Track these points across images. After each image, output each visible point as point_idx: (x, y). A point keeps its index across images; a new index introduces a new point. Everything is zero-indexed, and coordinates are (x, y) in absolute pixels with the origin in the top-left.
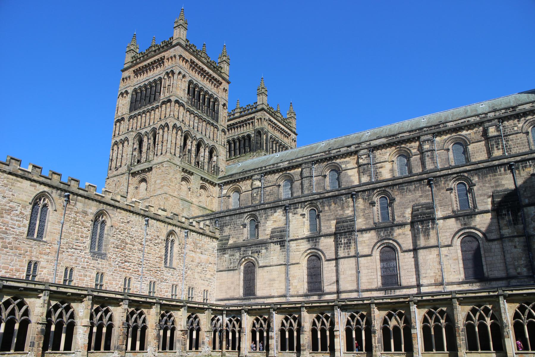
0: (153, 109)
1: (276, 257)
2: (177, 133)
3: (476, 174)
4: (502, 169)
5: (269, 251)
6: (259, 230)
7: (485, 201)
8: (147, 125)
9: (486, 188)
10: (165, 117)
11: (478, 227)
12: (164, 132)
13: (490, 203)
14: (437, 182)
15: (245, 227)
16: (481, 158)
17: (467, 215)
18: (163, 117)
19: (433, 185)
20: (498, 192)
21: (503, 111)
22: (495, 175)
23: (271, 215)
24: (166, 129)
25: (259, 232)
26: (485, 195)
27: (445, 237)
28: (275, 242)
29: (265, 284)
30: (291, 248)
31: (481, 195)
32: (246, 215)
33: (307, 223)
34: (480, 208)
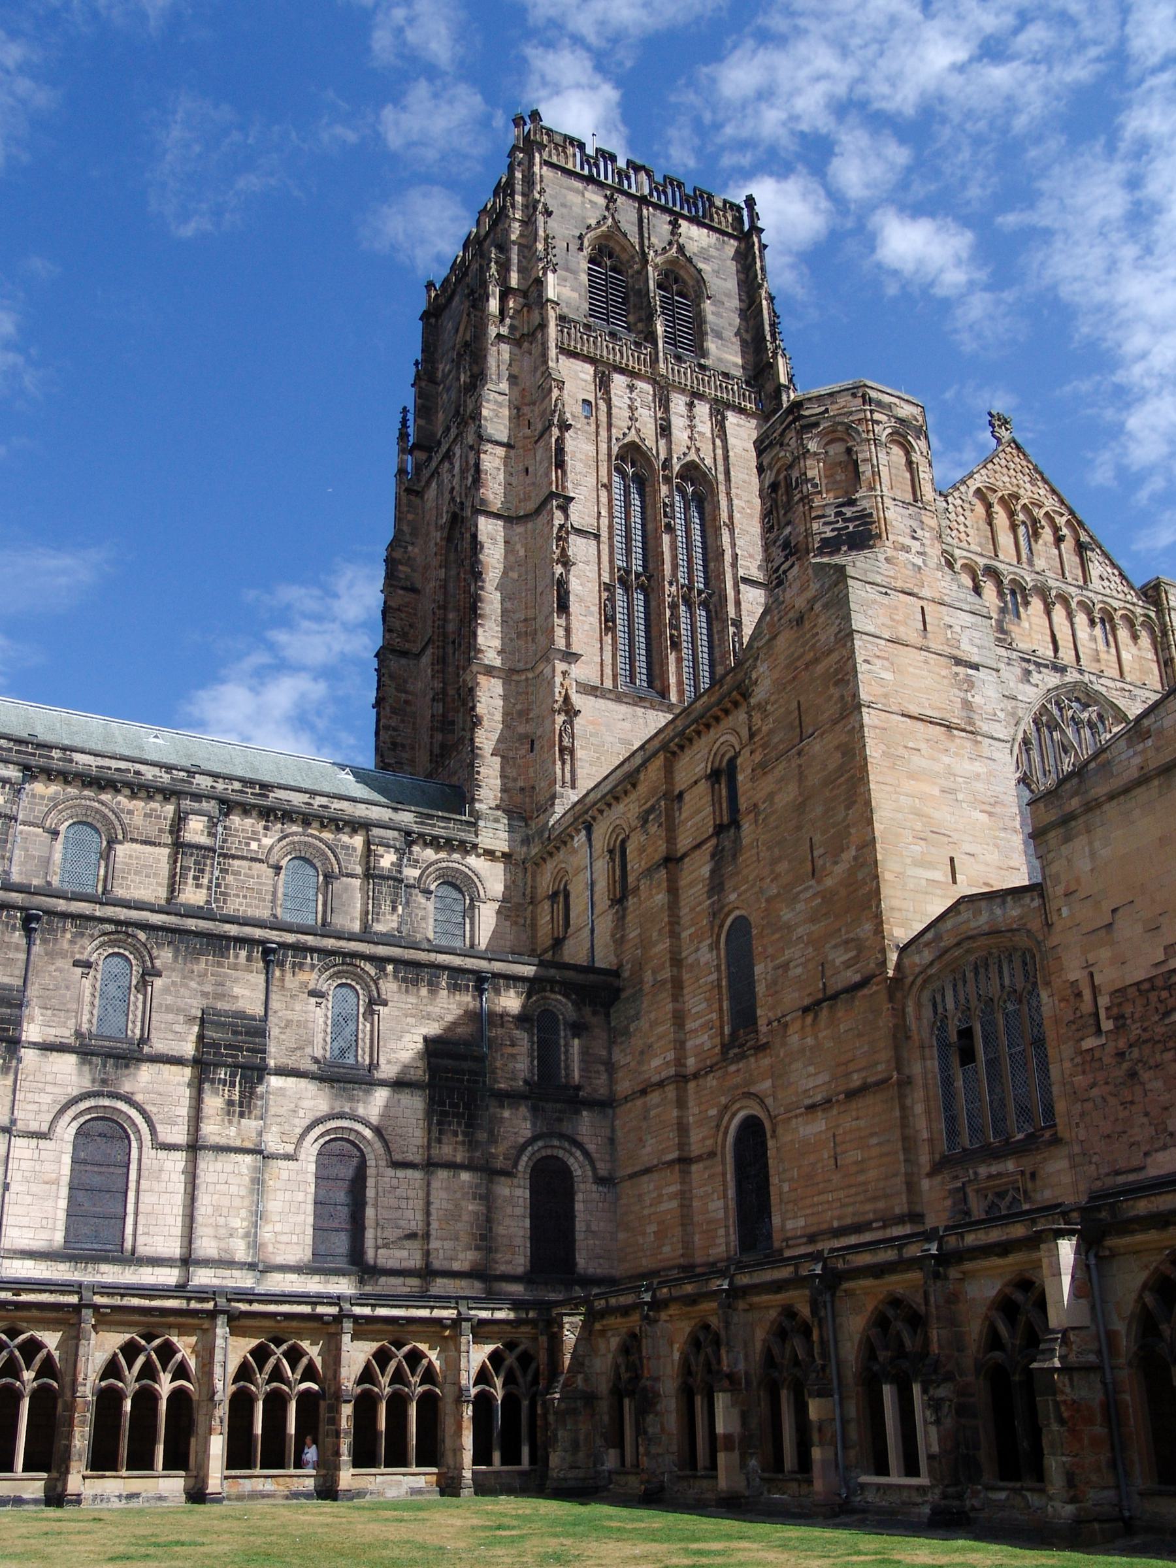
3: (170, 943)
4: (243, 954)
7: (177, 1028)
9: (186, 993)
11: (139, 1098)
13: (193, 1038)
14: (52, 931)
17: (117, 1057)
19: (37, 936)
20: (218, 1013)
26: (179, 1011)
27: (35, 1107)
31: (169, 1009)
34: (159, 1045)
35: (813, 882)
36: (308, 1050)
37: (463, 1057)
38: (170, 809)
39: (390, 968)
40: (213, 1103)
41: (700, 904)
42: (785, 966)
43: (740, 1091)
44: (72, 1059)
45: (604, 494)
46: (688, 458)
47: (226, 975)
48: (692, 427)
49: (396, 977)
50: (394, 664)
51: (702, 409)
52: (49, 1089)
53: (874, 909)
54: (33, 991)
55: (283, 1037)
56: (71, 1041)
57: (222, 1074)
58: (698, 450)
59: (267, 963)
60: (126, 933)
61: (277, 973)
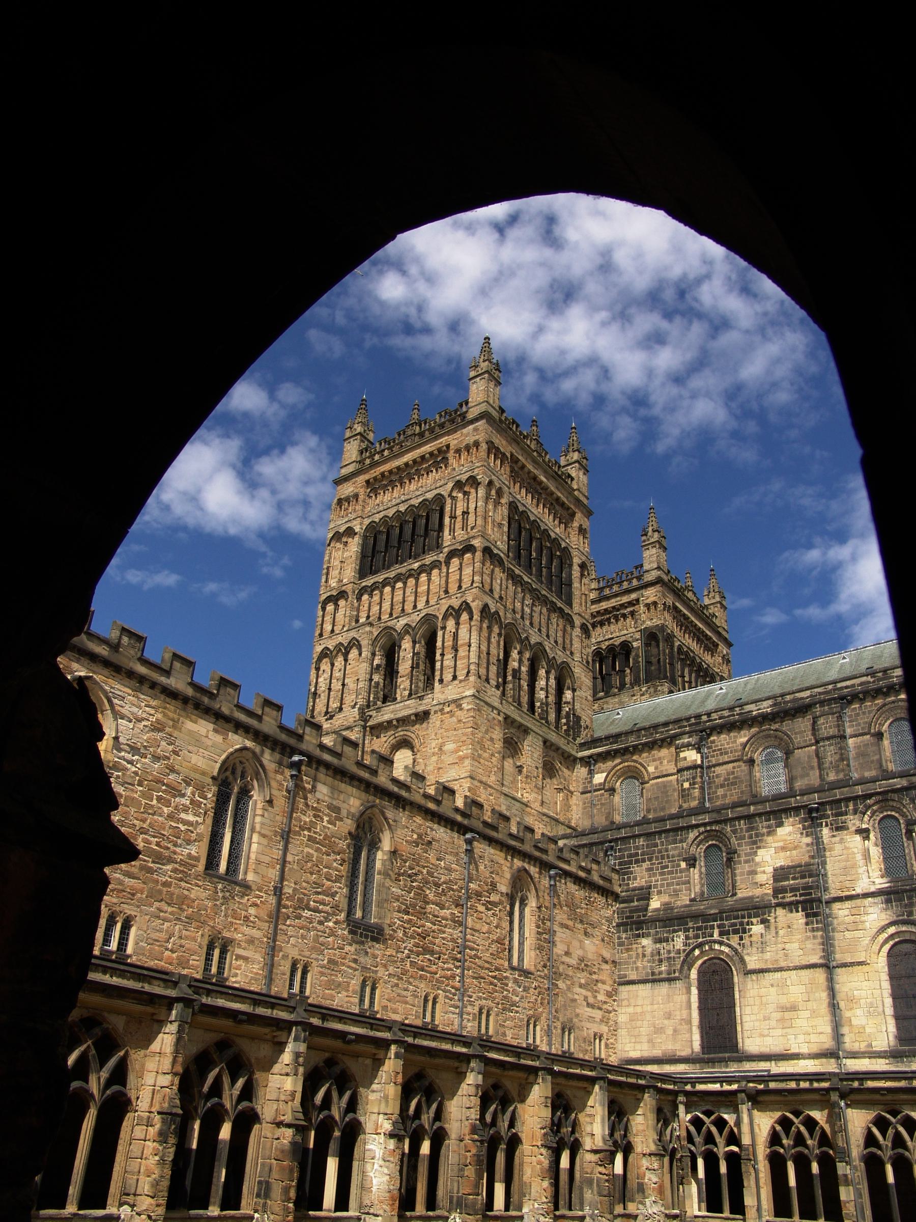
0: (422, 569)
1: (796, 945)
2: (490, 628)
5: (772, 928)
6: (737, 872)
8: (409, 607)
10: (460, 587)
12: (458, 624)
15: (694, 866)
18: (453, 588)
23: (769, 833)
24: (465, 616)
25: (738, 878)
28: (790, 904)
29: (766, 1018)
30: (835, 922)
32: (692, 835)
33: (876, 852)
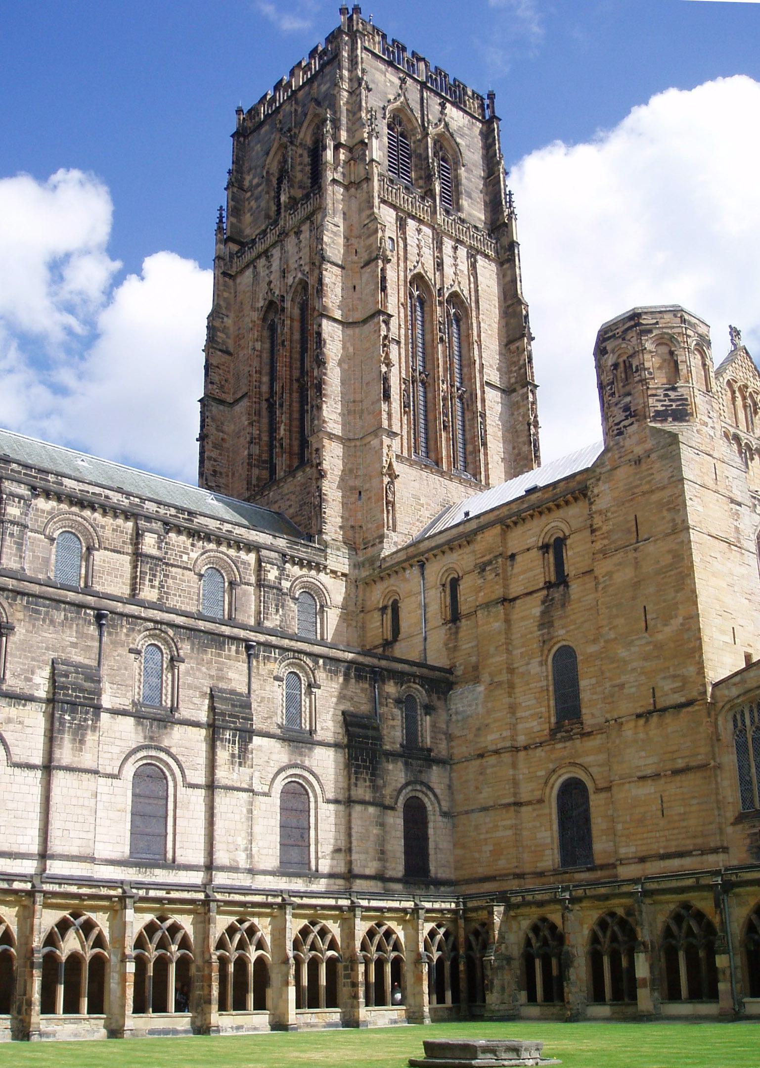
4: (234, 648)
7: (195, 700)
11: (173, 750)
13: (206, 708)
16: (113, 588)
17: (159, 720)
20: (221, 691)
21: (173, 511)
22: (220, 655)
26: (196, 688)
31: (190, 687)
34: (185, 712)
35: (646, 635)
36: (275, 719)
37: (365, 727)
38: (130, 524)
39: (321, 661)
40: (223, 755)
41: (531, 633)
42: (622, 686)
43: (567, 761)
44: (131, 721)
45: (402, 310)
46: (453, 289)
47: (224, 663)
48: (456, 265)
49: (325, 669)
50: (215, 409)
51: (462, 252)
52: (118, 742)
53: (697, 658)
54: (104, 671)
55: (259, 709)
56: (130, 708)
57: (228, 735)
58: (459, 283)
59: (249, 656)
60: (160, 630)
61: (255, 663)
